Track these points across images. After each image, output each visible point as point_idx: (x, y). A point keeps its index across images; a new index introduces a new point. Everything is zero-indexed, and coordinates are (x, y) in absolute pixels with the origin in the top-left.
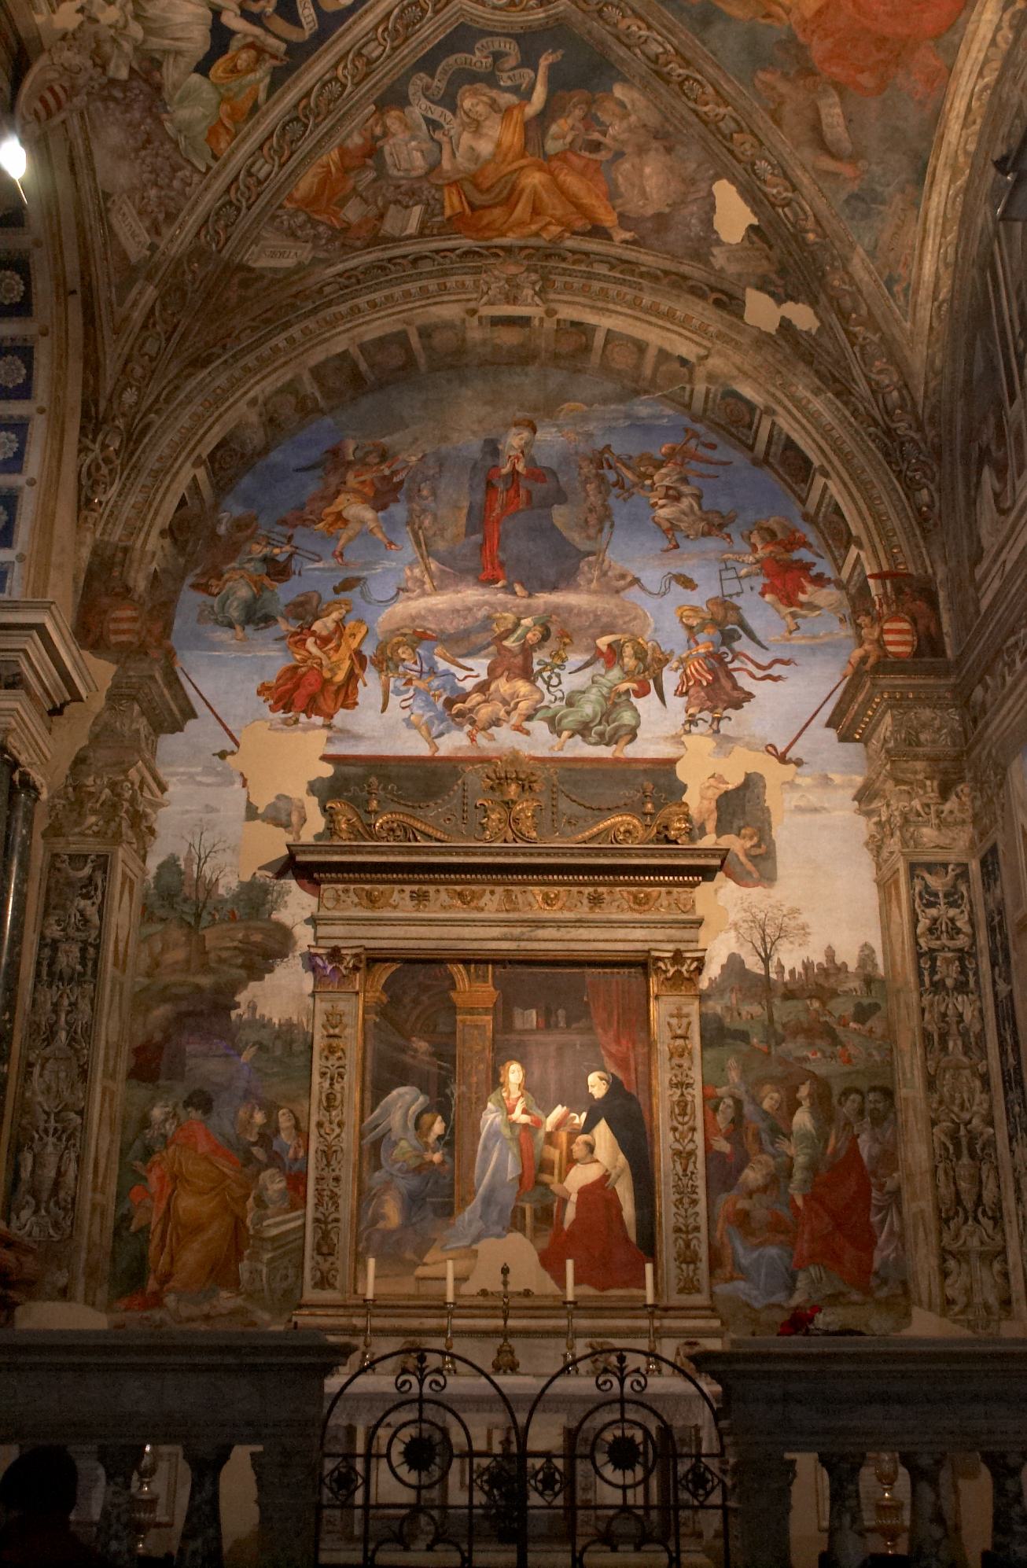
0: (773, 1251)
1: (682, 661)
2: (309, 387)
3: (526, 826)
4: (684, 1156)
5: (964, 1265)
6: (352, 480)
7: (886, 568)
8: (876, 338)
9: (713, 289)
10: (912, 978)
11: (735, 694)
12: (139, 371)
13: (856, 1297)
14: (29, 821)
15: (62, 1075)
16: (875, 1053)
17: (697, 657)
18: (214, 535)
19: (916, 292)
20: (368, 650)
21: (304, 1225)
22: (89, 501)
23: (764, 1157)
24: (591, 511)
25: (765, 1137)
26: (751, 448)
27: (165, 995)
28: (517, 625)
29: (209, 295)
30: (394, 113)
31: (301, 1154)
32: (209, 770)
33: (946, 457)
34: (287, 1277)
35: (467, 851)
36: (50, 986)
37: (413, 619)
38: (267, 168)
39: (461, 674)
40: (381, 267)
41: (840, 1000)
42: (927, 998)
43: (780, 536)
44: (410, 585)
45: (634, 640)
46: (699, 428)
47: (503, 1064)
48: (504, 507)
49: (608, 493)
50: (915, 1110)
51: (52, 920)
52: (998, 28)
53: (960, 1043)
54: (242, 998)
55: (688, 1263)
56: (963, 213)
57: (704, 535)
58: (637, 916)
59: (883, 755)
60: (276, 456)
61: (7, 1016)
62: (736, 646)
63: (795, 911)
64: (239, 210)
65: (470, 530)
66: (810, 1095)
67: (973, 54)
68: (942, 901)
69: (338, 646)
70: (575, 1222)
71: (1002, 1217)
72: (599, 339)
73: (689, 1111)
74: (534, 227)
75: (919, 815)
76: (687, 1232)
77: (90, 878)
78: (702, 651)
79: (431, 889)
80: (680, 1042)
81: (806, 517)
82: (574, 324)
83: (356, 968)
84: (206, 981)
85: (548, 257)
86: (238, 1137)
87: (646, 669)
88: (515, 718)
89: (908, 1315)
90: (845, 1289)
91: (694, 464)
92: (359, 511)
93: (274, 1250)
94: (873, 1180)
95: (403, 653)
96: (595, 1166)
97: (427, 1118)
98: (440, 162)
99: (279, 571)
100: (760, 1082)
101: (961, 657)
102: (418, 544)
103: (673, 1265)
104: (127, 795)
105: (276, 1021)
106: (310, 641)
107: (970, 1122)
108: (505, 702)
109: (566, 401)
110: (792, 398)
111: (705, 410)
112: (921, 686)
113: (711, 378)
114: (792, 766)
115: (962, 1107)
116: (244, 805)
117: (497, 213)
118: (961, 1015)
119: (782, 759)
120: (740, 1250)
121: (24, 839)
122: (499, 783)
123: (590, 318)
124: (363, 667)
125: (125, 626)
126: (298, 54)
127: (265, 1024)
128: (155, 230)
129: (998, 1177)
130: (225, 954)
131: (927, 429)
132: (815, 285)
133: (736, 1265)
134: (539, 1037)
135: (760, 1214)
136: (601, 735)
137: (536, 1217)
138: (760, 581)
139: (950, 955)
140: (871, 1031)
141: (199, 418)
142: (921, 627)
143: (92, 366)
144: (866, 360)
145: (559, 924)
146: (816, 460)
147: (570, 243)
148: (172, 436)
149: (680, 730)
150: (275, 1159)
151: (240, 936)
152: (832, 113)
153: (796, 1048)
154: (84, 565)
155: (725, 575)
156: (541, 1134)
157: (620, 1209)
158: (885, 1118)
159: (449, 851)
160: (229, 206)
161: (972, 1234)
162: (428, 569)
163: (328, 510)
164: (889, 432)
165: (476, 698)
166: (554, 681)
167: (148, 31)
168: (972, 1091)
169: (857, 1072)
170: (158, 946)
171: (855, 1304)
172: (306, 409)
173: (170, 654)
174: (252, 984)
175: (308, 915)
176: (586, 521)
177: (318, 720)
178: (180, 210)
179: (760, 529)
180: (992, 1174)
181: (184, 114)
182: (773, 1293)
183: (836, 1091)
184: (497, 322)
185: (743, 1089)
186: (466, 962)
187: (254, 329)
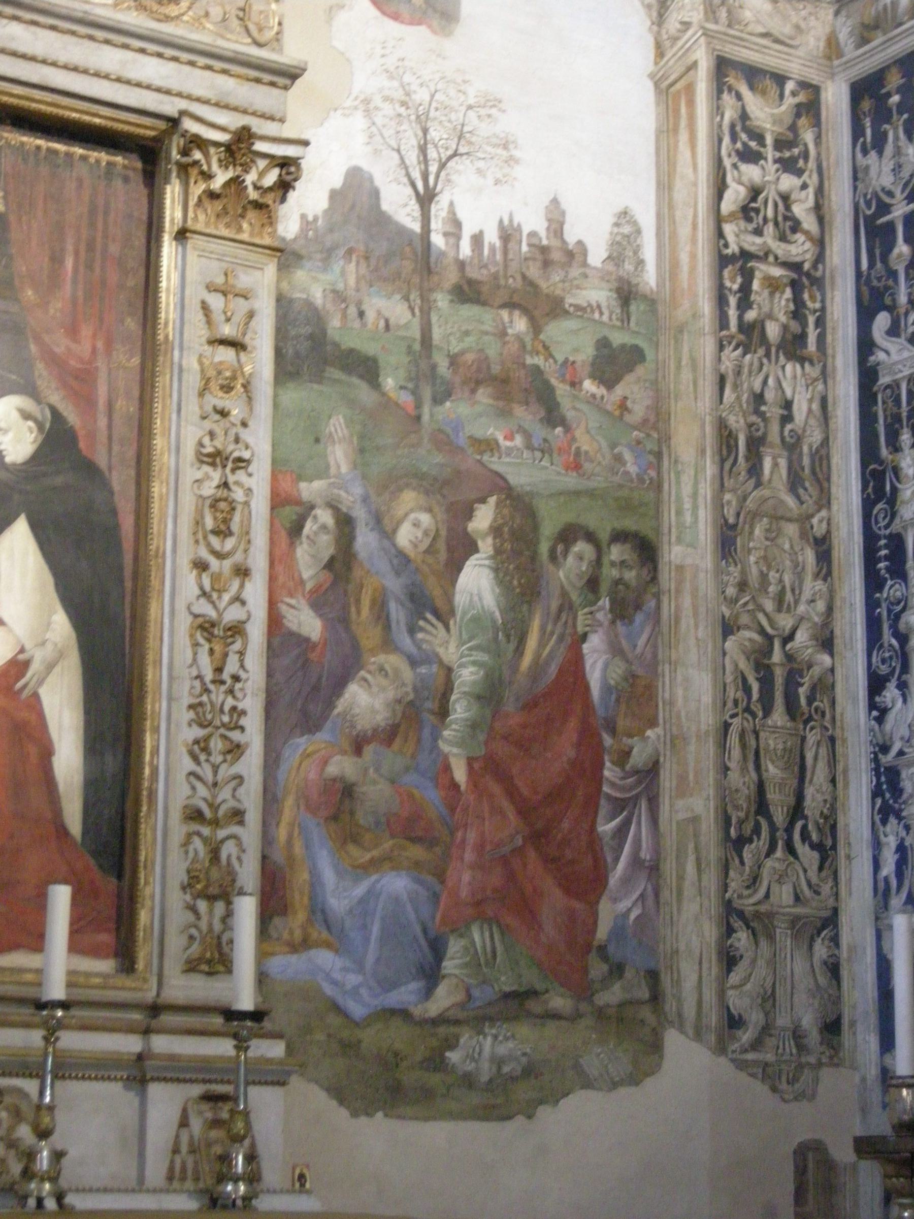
5: (763, 943)
10: (706, 307)
13: (559, 1002)
16: (628, 456)
23: (392, 661)
25: (397, 613)
41: (570, 324)
42: (731, 356)
53: (783, 463)
55: (211, 899)
66: (496, 531)
71: (834, 847)
73: (235, 526)
76: (215, 823)
80: (226, 355)
89: (656, 1047)
90: (539, 986)
94: (608, 740)
103: (177, 899)
107: (791, 637)
118: (788, 405)
120: (329, 876)
139: (777, 272)
140: (623, 406)
158: (638, 607)
168: (799, 571)
169: (591, 494)
171: (556, 1016)
180: (823, 751)
182: (394, 985)
183: (548, 529)
185: (358, 490)
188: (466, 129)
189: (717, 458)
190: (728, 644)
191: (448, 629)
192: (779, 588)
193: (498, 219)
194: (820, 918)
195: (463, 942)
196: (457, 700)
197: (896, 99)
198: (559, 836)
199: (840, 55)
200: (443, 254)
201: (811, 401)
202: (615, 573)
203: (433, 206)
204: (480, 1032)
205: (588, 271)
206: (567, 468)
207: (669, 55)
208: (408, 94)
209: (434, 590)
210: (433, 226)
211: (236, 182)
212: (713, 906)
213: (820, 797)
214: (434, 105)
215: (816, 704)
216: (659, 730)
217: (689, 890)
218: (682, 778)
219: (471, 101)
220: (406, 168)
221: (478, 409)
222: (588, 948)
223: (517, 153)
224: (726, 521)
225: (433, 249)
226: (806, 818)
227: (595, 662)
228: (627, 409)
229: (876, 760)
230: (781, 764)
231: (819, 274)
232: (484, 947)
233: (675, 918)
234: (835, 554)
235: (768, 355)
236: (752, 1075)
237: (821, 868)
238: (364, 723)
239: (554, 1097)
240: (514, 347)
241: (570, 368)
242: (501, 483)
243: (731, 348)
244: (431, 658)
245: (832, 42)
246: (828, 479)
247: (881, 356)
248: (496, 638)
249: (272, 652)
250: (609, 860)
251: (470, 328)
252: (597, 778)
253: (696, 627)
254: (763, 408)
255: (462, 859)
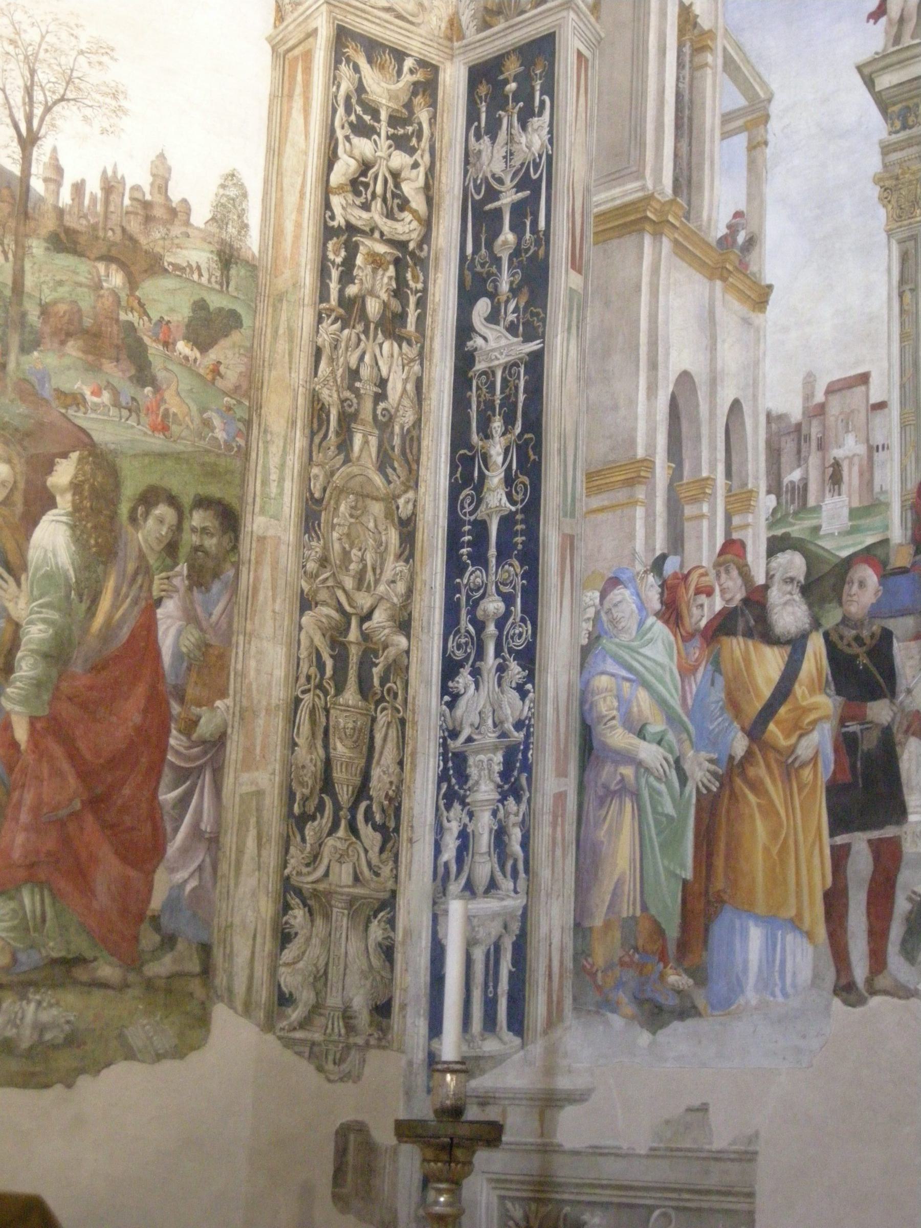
5: (319, 921)
10: (308, 278)
13: (107, 971)
16: (217, 422)
41: (168, 283)
42: (329, 328)
50: (274, 568)
53: (373, 441)
66: (76, 487)
68: (383, 128)
71: (397, 830)
89: (203, 1021)
90: (89, 954)
107: (368, 616)
115: (360, 578)
118: (383, 383)
139: (381, 249)
140: (216, 371)
158: (216, 575)
169: (178, 457)
171: (104, 985)
180: (393, 733)
183: (130, 489)
188: (75, 74)
189: (307, 431)
190: (304, 620)
191: (19, 584)
192: (361, 566)
193: (101, 169)
194: (378, 899)
195: (12, 905)
196: (23, 658)
197: (513, 86)
198: (119, 802)
199: (461, 37)
200: (41, 199)
201: (406, 381)
202: (195, 539)
203: (35, 149)
204: (23, 997)
205: (190, 231)
206: (154, 429)
207: (289, 20)
208: (18, 33)
210: (34, 170)
212: (272, 882)
213: (386, 779)
214: (44, 46)
215: (389, 685)
216: (229, 701)
218: (249, 750)
219: (83, 46)
220: (10, 108)
221: (67, 361)
223: (123, 103)
224: (312, 494)
225: (31, 195)
226: (370, 798)
227: (168, 629)
228: (219, 374)
229: (444, 745)
230: (349, 743)
231: (423, 254)
232: (34, 912)
233: (231, 892)
234: (419, 536)
235: (366, 332)
236: (299, 1054)
237: (382, 850)
239: (96, 1067)
240: (108, 302)
241: (164, 327)
242: (87, 440)
243: (330, 321)
245: (454, 24)
246: (418, 462)
247: (479, 341)
248: (68, 596)
250: (169, 829)
251: (64, 278)
252: (162, 747)
253: (274, 600)
254: (358, 384)
255: (16, 820)
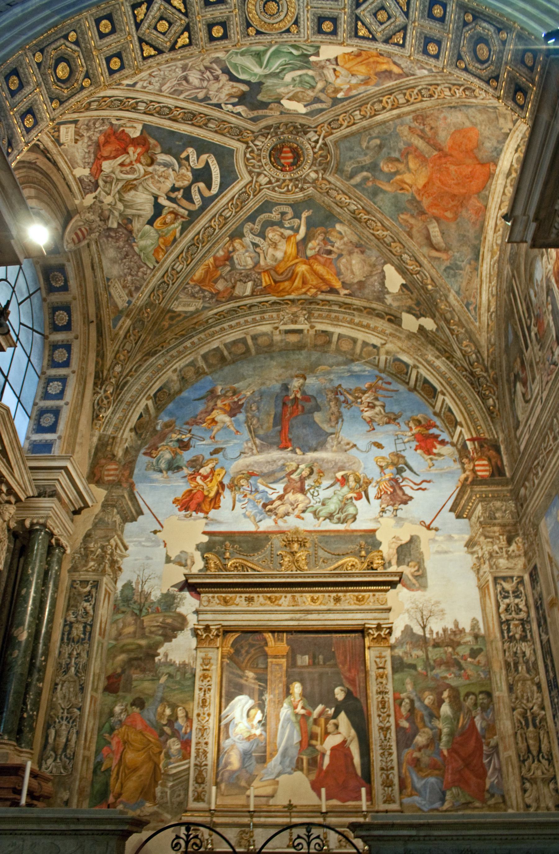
0: (432, 780)
1: (378, 483)
2: (201, 363)
3: (302, 564)
4: (385, 730)
6: (219, 404)
7: (474, 436)
8: (463, 331)
9: (387, 314)
10: (498, 635)
11: (404, 497)
12: (122, 357)
13: (477, 804)
14: (60, 563)
15: (72, 689)
16: (481, 674)
17: (385, 480)
18: (155, 431)
19: (480, 309)
20: (226, 482)
21: (189, 768)
22: (98, 416)
23: (426, 730)
24: (332, 414)
25: (426, 719)
26: (408, 383)
27: (123, 650)
28: (298, 468)
29: (155, 324)
30: (237, 241)
31: (188, 731)
32: (148, 539)
33: (500, 383)
34: (179, 795)
35: (272, 576)
36: (68, 646)
37: (248, 466)
38: (181, 266)
39: (270, 491)
40: (234, 310)
42: (506, 645)
43: (423, 423)
44: (246, 450)
45: (354, 473)
46: (383, 375)
47: (291, 683)
48: (291, 414)
49: (340, 406)
50: (503, 703)
51: (71, 612)
52: (505, 187)
54: (161, 651)
55: (388, 787)
56: (498, 272)
57: (387, 423)
58: (357, 607)
59: (478, 524)
60: (185, 394)
61: (43, 658)
62: (404, 474)
63: (437, 603)
64: (168, 285)
65: (275, 425)
66: (449, 697)
67: (495, 199)
68: (511, 595)
69: (211, 480)
70: (329, 766)
72: (335, 338)
74: (304, 290)
75: (497, 553)
76: (387, 770)
77: (90, 592)
78: (387, 477)
79: (255, 596)
80: (381, 671)
81: (435, 414)
82: (323, 332)
83: (217, 636)
84: (143, 642)
85: (311, 303)
86: (157, 721)
87: (360, 487)
88: (297, 512)
91: (381, 392)
92: (222, 417)
93: (174, 780)
94: (483, 740)
95: (243, 482)
96: (339, 736)
97: (252, 712)
98: (259, 262)
99: (184, 446)
100: (423, 691)
101: (513, 478)
102: (250, 432)
103: (380, 788)
104: (109, 552)
105: (177, 662)
106: (198, 479)
107: (532, 708)
108: (292, 504)
109: (319, 365)
110: (426, 361)
111: (385, 367)
112: (496, 491)
113: (387, 353)
114: (433, 531)
115: (528, 700)
116: (164, 556)
117: (287, 284)
118: (524, 653)
119: (428, 528)
120: (415, 779)
121: (57, 571)
122: (289, 543)
123: (330, 329)
124: (223, 489)
125: (112, 472)
126: (193, 216)
127: (172, 664)
128: (130, 294)
129: (549, 737)
130: (153, 629)
131: (490, 371)
132: (433, 309)
133: (414, 788)
134: (310, 670)
135: (425, 760)
136: (339, 519)
137: (309, 764)
138: (414, 444)
139: (517, 622)
141: (150, 379)
142: (493, 463)
143: (101, 355)
144: (460, 342)
145: (319, 612)
146: (439, 388)
147: (321, 296)
148: (137, 387)
149: (377, 515)
150: (175, 733)
151: (161, 620)
152: (435, 230)
153: (440, 672)
154: (94, 445)
155: (397, 441)
156: (311, 720)
157: (352, 759)
159: (263, 576)
160: (163, 284)
161: (537, 769)
162: (255, 443)
163: (209, 417)
164: (472, 374)
165: (278, 503)
166: (316, 494)
167: (126, 206)
169: (473, 684)
170: (121, 625)
171: (477, 808)
172: (199, 373)
173: (132, 486)
174: (166, 644)
175: (194, 609)
176: (330, 419)
177: (201, 515)
178: (141, 286)
179: (414, 420)
181: (142, 243)
184: (288, 332)
186: (273, 632)
187: (176, 339)
209: (435, 712)
211: (379, 635)
217: (510, 774)
222: (484, 791)
238: (421, 744)
244: (436, 728)
249: (397, 732)
